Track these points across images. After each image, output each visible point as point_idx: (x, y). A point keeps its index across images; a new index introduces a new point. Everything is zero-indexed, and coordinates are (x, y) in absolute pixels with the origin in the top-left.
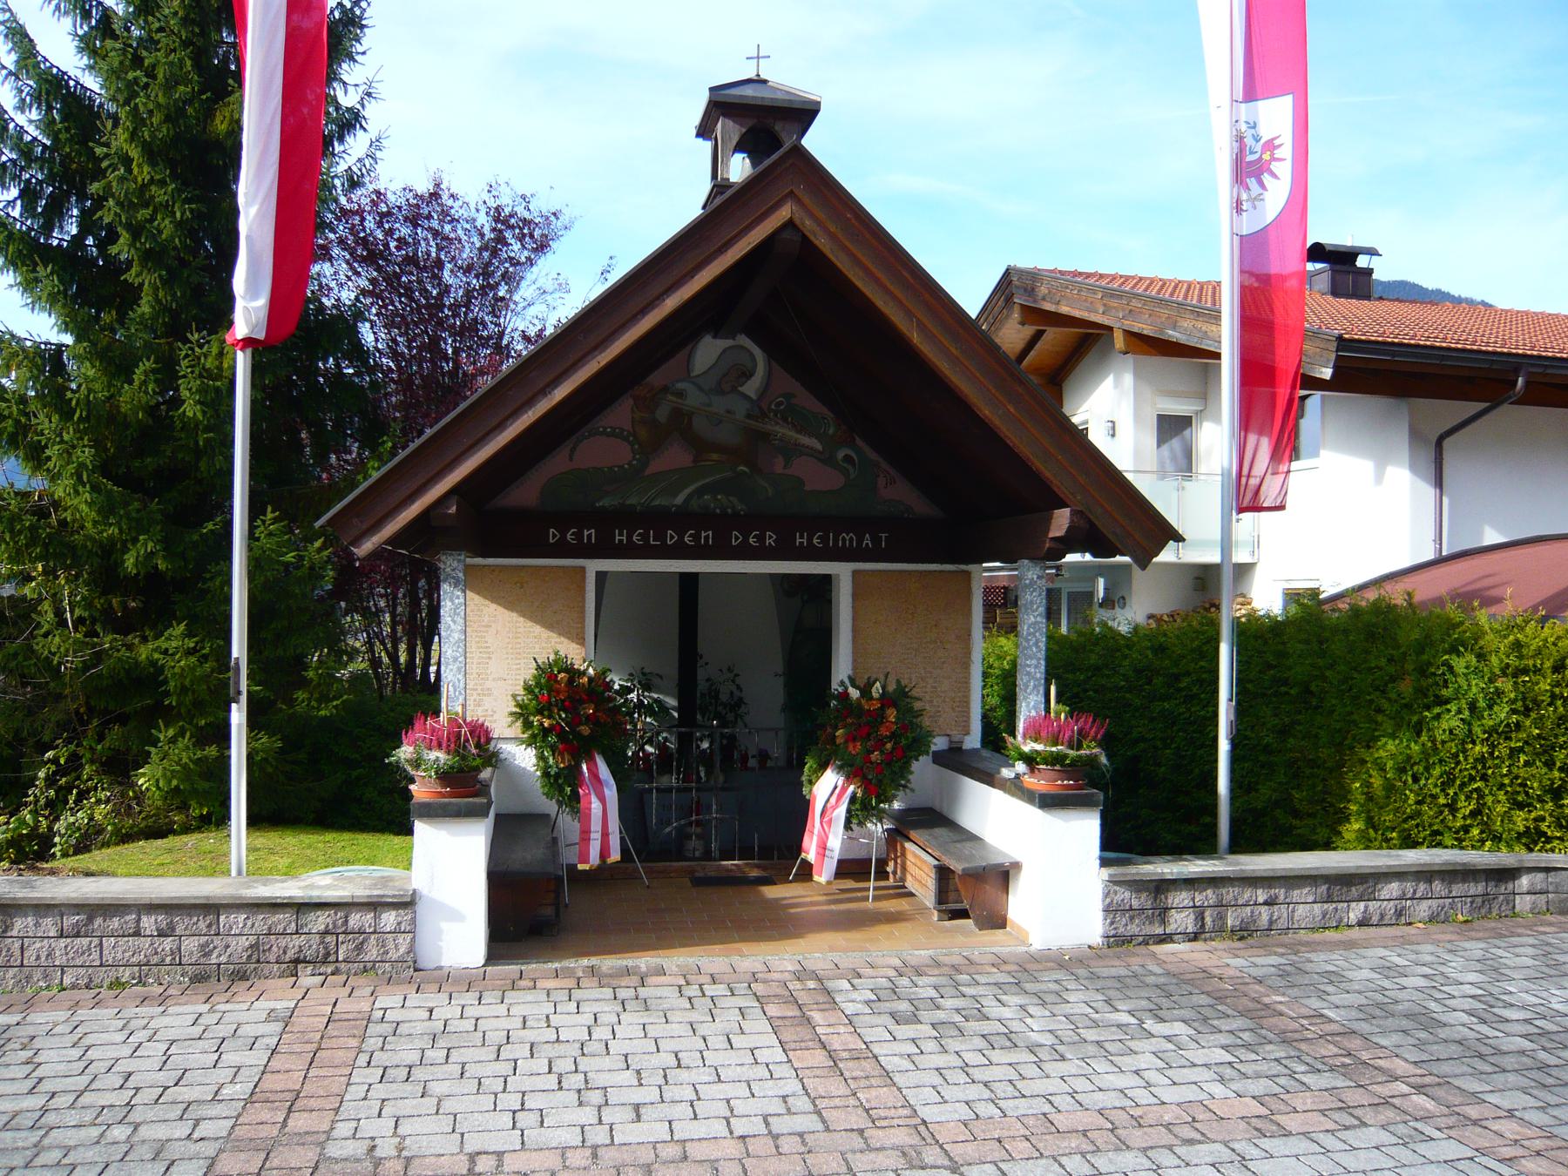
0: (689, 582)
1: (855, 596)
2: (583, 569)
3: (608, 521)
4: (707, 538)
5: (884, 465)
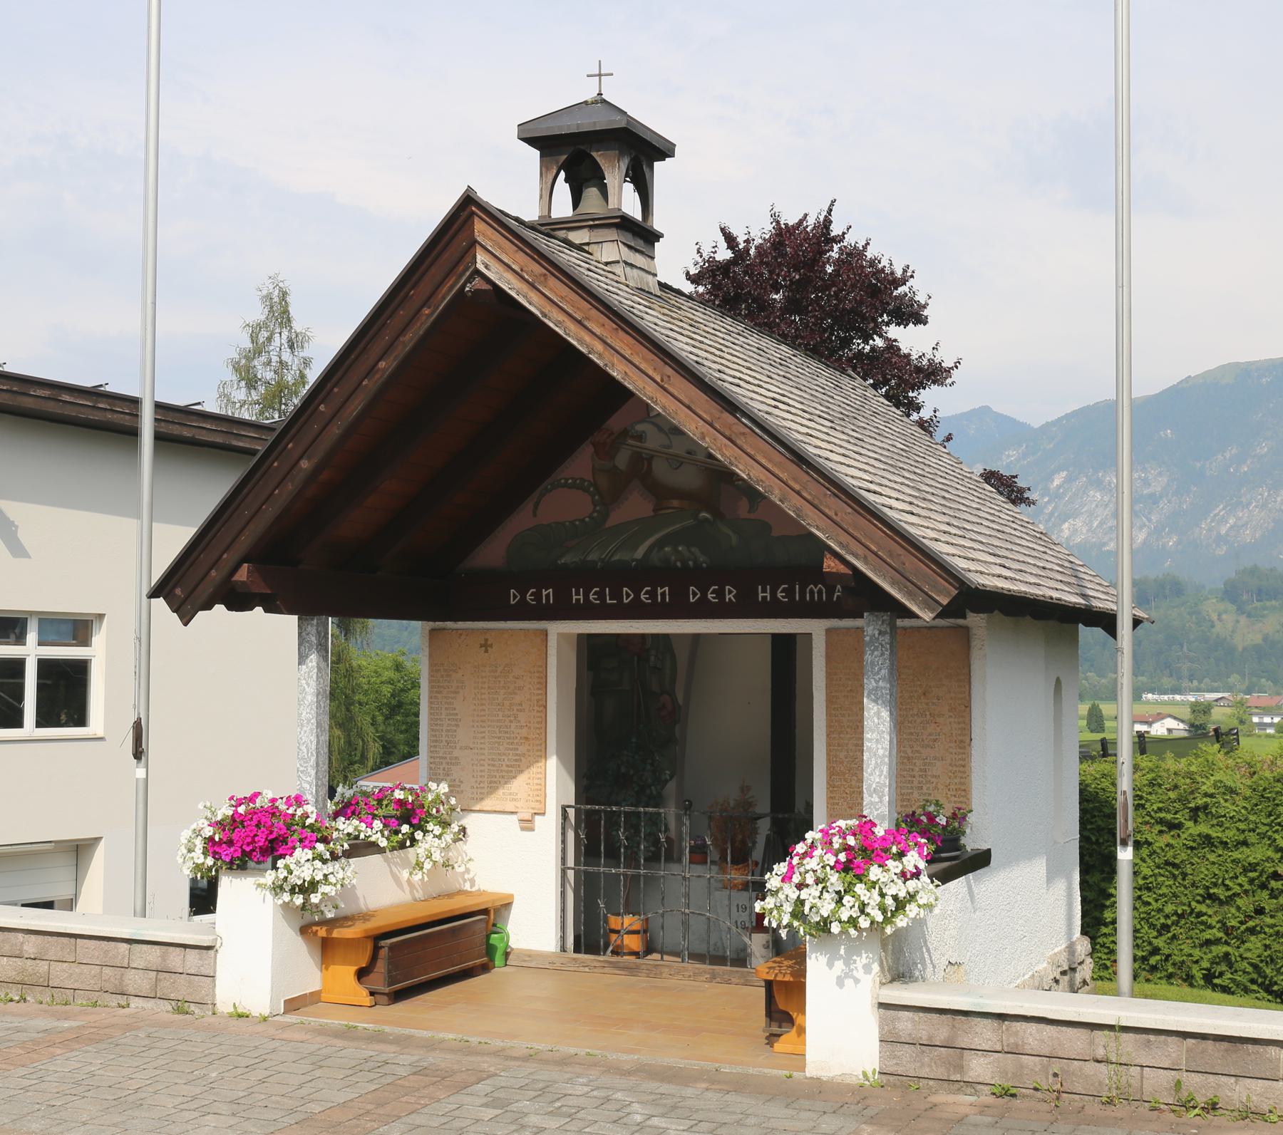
2: (545, 633)
3: (564, 579)
4: (663, 594)
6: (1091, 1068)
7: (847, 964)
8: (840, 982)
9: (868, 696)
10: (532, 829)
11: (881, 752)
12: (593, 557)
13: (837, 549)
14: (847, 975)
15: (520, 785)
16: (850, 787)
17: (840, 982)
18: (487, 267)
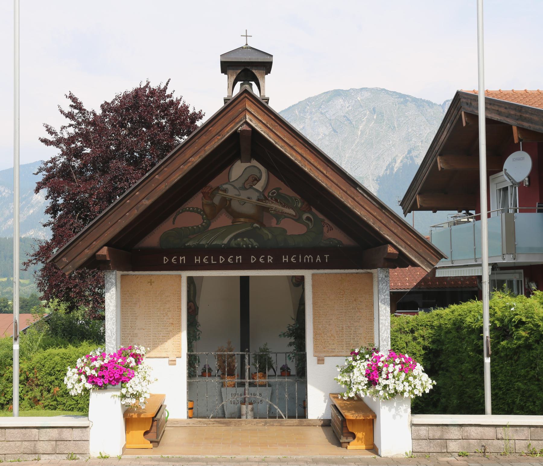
0: (245, 280)
1: (313, 286)
2: (180, 276)
4: (239, 259)
5: (327, 221)
6: (496, 442)
7: (397, 409)
8: (394, 417)
9: (381, 302)
10: (175, 364)
11: (387, 324)
12: (203, 242)
13: (395, 244)
14: (397, 414)
15: (169, 344)
16: (324, 339)
17: (394, 417)
18: (251, 120)
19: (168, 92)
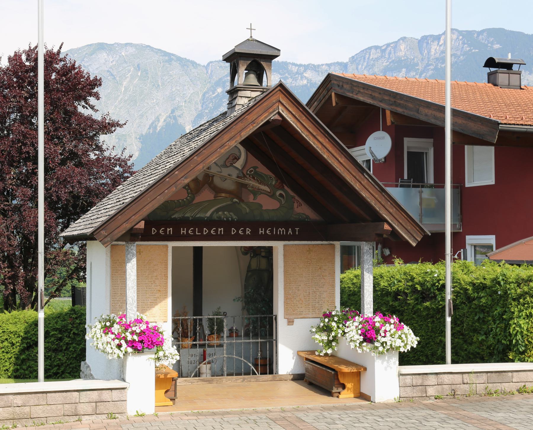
1: (285, 256)
2: (167, 246)
3: (178, 224)
4: (221, 231)
5: (297, 198)
6: (462, 386)
7: (388, 363)
8: (386, 369)
12: (187, 215)
13: (390, 222)
17: (386, 369)
18: (283, 111)
19: (61, 56)
